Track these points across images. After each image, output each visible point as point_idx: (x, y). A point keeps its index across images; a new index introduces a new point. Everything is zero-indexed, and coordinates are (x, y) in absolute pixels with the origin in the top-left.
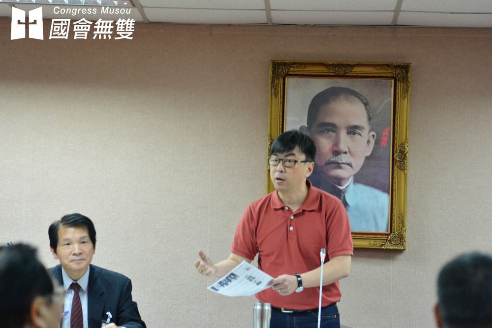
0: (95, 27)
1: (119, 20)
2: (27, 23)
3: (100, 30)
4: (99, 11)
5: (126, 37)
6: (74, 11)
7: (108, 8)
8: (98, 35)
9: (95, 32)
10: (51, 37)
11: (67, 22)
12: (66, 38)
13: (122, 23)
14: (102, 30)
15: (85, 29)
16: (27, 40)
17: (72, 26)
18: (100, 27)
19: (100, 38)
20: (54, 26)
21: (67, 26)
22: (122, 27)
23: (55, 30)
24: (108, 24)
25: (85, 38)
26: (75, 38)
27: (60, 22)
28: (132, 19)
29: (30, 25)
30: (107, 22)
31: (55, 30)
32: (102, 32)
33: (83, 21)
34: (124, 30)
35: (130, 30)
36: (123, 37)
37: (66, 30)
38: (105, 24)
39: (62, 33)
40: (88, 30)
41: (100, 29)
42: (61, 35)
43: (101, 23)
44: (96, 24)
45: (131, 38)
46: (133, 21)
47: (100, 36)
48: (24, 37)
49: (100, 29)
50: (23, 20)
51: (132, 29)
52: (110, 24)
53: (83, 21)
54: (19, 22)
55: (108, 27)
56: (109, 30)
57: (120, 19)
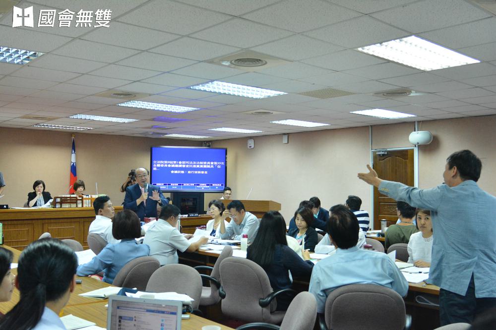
1: (98, 11)
5: (104, 25)
8: (80, 23)
10: (39, 25)
12: (53, 26)
13: (101, 13)
15: (68, 19)
17: (57, 16)
18: (82, 17)
22: (100, 17)
25: (69, 26)
26: (60, 26)
28: (109, 10)
29: (21, 15)
30: (87, 12)
31: (42, 19)
32: (83, 21)
33: (67, 12)
34: (102, 19)
35: (107, 19)
36: (101, 25)
37: (52, 19)
38: (86, 13)
39: (49, 22)
40: (71, 19)
42: (49, 24)
43: (82, 15)
44: (78, 14)
45: (108, 26)
46: (109, 11)
47: (81, 24)
51: (109, 18)
55: (88, 17)
56: (90, 19)
57: (99, 10)
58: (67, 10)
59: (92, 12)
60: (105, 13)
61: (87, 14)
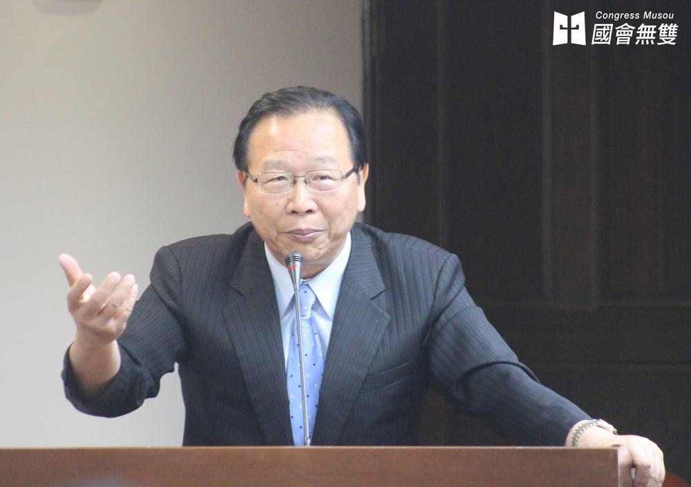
0: (638, 32)
2: (569, 29)
3: (642, 36)
4: (642, 15)
5: (669, 42)
6: (617, 16)
7: (650, 12)
8: (641, 40)
9: (637, 38)
10: (593, 43)
11: (610, 27)
12: (609, 43)
14: (644, 35)
15: (627, 35)
16: (570, 46)
17: (614, 32)
19: (643, 43)
20: (596, 31)
21: (609, 31)
22: (665, 32)
23: (597, 35)
24: (651, 28)
25: (628, 43)
26: (618, 43)
27: (602, 27)
29: (572, 30)
30: (649, 27)
31: (597, 35)
32: (644, 37)
33: (626, 27)
35: (673, 35)
36: (666, 42)
37: (608, 36)
39: (604, 38)
40: (631, 35)
41: (643, 34)
42: (604, 41)
43: (644, 28)
44: (639, 29)
45: (674, 44)
46: (675, 26)
48: (566, 42)
49: (643, 34)
50: (565, 25)
52: (653, 29)
53: (626, 27)
54: (561, 26)
56: (652, 35)
58: (626, 24)
59: (655, 26)
60: (670, 28)
61: (649, 29)
